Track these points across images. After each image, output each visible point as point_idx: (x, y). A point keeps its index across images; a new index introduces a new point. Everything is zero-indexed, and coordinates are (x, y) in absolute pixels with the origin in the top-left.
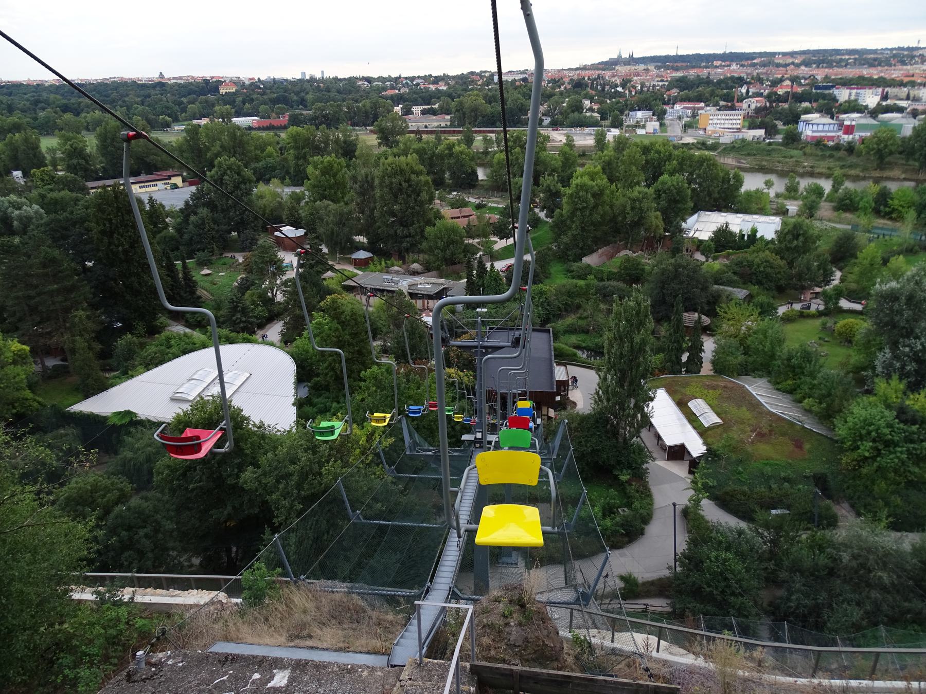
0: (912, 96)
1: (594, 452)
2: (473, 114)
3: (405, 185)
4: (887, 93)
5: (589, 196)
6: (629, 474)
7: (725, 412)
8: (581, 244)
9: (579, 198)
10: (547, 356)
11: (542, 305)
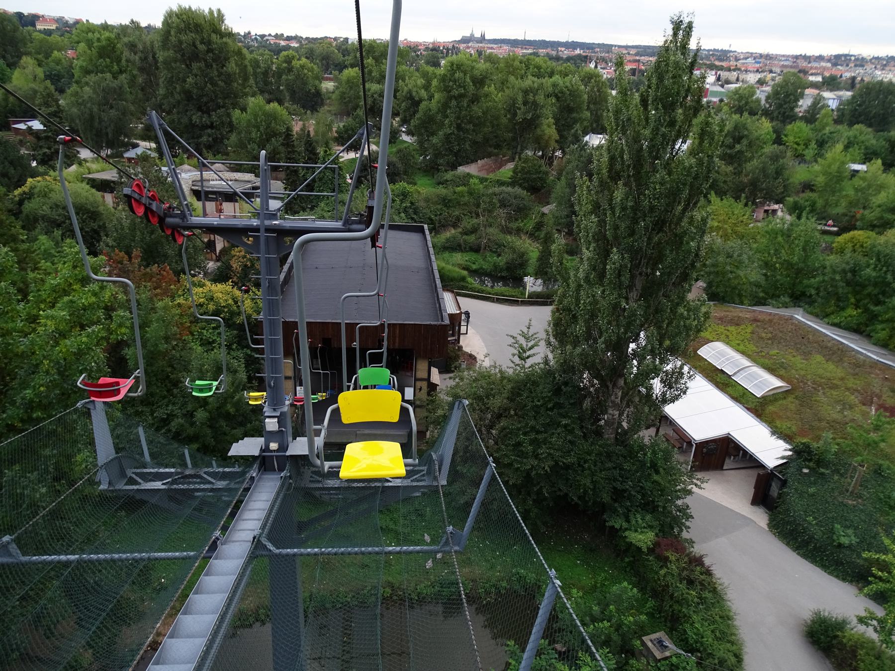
0: (741, 79)
1: (560, 470)
2: (324, 62)
3: (202, 47)
4: (720, 75)
5: (468, 80)
6: (651, 527)
7: (782, 366)
8: (456, 148)
9: (455, 81)
10: (421, 263)
11: (405, 210)
